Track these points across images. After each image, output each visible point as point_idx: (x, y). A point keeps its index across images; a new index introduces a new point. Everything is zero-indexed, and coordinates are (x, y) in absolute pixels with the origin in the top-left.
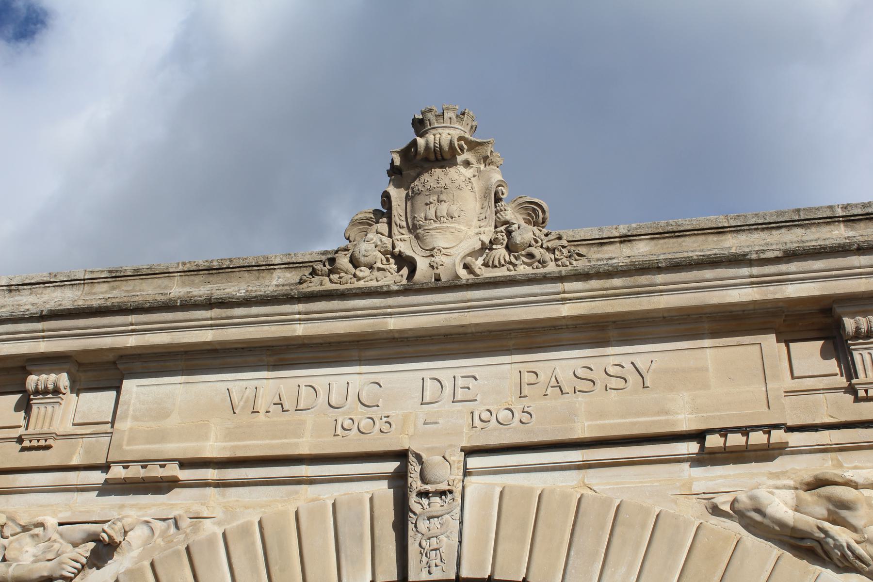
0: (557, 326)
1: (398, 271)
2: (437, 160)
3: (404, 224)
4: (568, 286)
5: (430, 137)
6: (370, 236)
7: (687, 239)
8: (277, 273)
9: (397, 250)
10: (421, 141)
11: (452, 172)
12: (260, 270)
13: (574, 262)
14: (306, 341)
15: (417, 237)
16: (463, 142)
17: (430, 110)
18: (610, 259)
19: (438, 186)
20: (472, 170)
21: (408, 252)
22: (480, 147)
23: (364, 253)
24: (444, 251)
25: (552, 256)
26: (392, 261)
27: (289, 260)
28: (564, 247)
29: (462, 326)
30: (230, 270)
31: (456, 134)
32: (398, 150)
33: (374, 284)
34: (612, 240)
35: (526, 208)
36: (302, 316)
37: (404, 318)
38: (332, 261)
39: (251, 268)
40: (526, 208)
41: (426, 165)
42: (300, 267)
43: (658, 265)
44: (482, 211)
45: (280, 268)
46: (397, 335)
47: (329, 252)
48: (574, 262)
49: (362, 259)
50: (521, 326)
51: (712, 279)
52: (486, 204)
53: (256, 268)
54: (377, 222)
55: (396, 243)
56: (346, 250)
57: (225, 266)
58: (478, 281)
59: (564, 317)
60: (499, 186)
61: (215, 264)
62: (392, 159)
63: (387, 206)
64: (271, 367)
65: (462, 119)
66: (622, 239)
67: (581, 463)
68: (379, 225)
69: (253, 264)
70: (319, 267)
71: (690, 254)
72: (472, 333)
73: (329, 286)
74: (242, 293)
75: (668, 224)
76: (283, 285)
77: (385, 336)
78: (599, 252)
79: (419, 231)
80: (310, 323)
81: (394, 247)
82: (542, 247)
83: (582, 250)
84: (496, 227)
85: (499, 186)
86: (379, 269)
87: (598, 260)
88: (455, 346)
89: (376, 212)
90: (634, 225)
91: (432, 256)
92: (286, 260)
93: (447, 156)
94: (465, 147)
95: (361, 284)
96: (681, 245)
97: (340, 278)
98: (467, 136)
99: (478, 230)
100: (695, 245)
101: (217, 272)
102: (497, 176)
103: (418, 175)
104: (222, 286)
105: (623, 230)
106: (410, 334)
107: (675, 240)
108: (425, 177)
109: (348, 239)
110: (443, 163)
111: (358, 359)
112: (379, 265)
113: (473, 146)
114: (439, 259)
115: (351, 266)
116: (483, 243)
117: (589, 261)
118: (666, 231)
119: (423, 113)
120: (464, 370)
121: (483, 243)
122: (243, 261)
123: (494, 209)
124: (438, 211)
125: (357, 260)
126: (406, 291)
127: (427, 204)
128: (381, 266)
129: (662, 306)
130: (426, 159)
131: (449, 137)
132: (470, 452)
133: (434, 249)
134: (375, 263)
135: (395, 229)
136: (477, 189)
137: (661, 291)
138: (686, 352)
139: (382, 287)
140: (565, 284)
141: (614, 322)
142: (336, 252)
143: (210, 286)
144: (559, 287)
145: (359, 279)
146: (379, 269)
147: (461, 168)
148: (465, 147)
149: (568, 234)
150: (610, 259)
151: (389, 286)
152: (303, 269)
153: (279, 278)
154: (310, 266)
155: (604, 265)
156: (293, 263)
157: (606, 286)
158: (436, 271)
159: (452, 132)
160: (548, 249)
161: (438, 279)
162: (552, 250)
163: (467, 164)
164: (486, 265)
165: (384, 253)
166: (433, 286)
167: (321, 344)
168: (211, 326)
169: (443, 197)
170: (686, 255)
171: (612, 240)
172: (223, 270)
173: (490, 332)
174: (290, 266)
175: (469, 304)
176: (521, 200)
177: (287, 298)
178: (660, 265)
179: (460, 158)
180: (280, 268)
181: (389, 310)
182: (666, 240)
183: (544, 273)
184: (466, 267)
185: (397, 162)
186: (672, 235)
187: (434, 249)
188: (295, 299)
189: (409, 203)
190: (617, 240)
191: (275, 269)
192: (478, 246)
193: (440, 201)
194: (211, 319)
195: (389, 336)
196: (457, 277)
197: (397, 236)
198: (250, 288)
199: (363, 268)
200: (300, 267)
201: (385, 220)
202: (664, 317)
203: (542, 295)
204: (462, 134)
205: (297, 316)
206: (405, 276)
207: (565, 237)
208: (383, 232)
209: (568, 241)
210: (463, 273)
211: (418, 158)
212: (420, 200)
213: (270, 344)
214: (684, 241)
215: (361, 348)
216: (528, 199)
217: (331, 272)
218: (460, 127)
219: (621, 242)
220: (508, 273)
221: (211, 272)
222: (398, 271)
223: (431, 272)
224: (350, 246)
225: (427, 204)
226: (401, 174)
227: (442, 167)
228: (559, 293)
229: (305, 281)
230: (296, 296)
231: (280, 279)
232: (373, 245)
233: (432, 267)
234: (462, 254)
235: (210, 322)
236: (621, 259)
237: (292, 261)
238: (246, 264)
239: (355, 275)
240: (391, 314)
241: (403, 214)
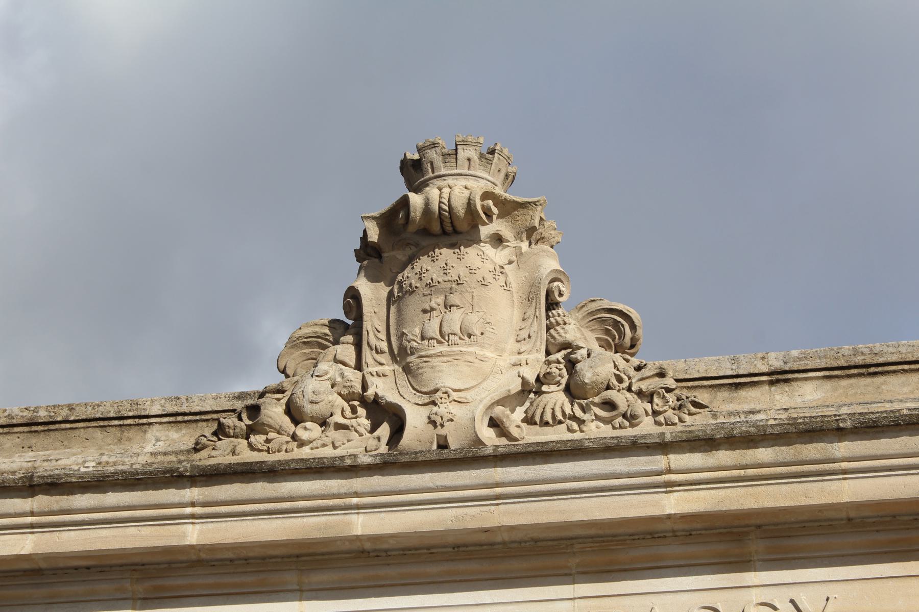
0: (657, 533)
1: (373, 430)
2: (444, 233)
3: (384, 346)
4: (677, 460)
5: (433, 192)
6: (323, 366)
7: (890, 379)
8: (155, 432)
9: (370, 393)
10: (416, 200)
11: (471, 254)
12: (123, 425)
13: (687, 418)
14: (203, 556)
15: (407, 370)
16: (490, 203)
17: (434, 145)
18: (752, 412)
19: (446, 278)
20: (506, 251)
21: (390, 396)
22: (521, 211)
23: (310, 396)
24: (454, 395)
25: (648, 407)
26: (362, 411)
27: (176, 409)
28: (669, 390)
29: (486, 530)
30: (68, 426)
31: (478, 187)
32: (375, 214)
33: (328, 452)
34: (756, 379)
35: (602, 321)
36: (198, 510)
37: (382, 515)
38: (254, 411)
39: (106, 423)
40: (602, 321)
41: (425, 242)
43: (838, 425)
44: (524, 325)
45: (161, 423)
46: (368, 546)
47: (250, 395)
48: (687, 418)
49: (308, 408)
50: (592, 532)
51: (771, 463)
52: (530, 312)
53: (116, 422)
54: (336, 342)
55: (369, 379)
56: (280, 390)
57: (59, 419)
58: (515, 449)
59: (669, 517)
60: (554, 280)
61: (43, 415)
62: (365, 231)
63: (354, 315)
64: (139, 602)
65: (490, 161)
66: (774, 378)
68: (339, 348)
69: (112, 415)
70: (230, 421)
71: (896, 406)
72: (504, 543)
73: (246, 456)
74: (90, 467)
75: (856, 352)
76: (165, 454)
77: (347, 546)
78: (731, 400)
79: (411, 359)
80: (212, 522)
81: (365, 387)
82: (629, 389)
83: (702, 397)
84: (548, 353)
85: (554, 280)
86: (339, 427)
87: (731, 414)
88: (474, 566)
89: (334, 324)
90: (795, 353)
91: (434, 403)
92: (170, 408)
93: (463, 226)
94: (495, 210)
95: (305, 452)
97: (268, 441)
98: (499, 191)
99: (515, 358)
100: (905, 390)
101: (46, 428)
102: (550, 263)
103: (411, 260)
104: (53, 454)
105: (775, 361)
106: (392, 543)
107: (869, 380)
108: (423, 262)
109: (283, 371)
110: (454, 239)
111: (297, 587)
112: (338, 418)
113: (508, 208)
114: (445, 409)
115: (287, 419)
116: (524, 382)
117: (715, 416)
118: (852, 363)
119: (420, 150)
121: (524, 382)
123: (544, 322)
124: (445, 324)
125: (299, 409)
126: (384, 467)
127: (425, 311)
128: (341, 420)
129: (846, 499)
130: (425, 232)
131: (466, 193)
133: (436, 391)
134: (331, 415)
135: (367, 355)
136: (514, 286)
137: (845, 472)
138: (891, 583)
139: (342, 458)
140: (671, 456)
141: (759, 527)
142: (262, 395)
143: (31, 454)
144: (659, 461)
145: (302, 444)
146: (339, 427)
147: (488, 249)
148: (495, 210)
149: (677, 367)
150: (752, 412)
151: (355, 456)
152: (200, 424)
153: (158, 440)
154: (214, 420)
155: (741, 424)
157: (744, 462)
158: (442, 432)
159: (471, 183)
160: (640, 393)
161: (443, 445)
162: (649, 397)
163: (498, 240)
164: (529, 420)
165: (348, 398)
166: (434, 457)
167: (231, 560)
168: (32, 526)
169: (454, 299)
170: (888, 407)
171: (756, 379)
172: (57, 426)
173: (536, 541)
174: (177, 418)
175: (499, 490)
176: (593, 306)
177: (172, 476)
178: (841, 425)
179: (485, 231)
180: (161, 423)
181: (355, 500)
182: (853, 381)
183: (634, 437)
184: (494, 423)
185: (374, 235)
186: (864, 370)
187: (436, 391)
188: (185, 480)
189: (393, 309)
190: (764, 378)
191: (150, 424)
192: (516, 386)
193: (448, 306)
194: (32, 514)
195: (356, 546)
196: (478, 442)
197: (371, 367)
198: (105, 459)
199: (309, 424)
200: (197, 421)
201: (349, 338)
202: (849, 520)
203: (629, 475)
204: (489, 187)
205: (189, 510)
206: (385, 440)
207: (670, 373)
208: (347, 360)
209: (677, 381)
210: (488, 435)
211: (411, 228)
212: (413, 304)
213: (137, 560)
214: (885, 383)
215: (304, 568)
216: (606, 304)
217: (251, 430)
218: (485, 175)
219: (771, 383)
220: (569, 436)
221: (34, 428)
222: (373, 430)
223: (431, 433)
224: (287, 384)
225: (425, 311)
226: (380, 257)
227: (452, 246)
228: (660, 473)
229: (204, 447)
230: (188, 474)
232: (328, 384)
233: (433, 423)
234: (487, 401)
235: (29, 520)
236: (772, 414)
237: (182, 411)
238: (98, 415)
239: (294, 437)
240: (358, 507)
241: (382, 328)
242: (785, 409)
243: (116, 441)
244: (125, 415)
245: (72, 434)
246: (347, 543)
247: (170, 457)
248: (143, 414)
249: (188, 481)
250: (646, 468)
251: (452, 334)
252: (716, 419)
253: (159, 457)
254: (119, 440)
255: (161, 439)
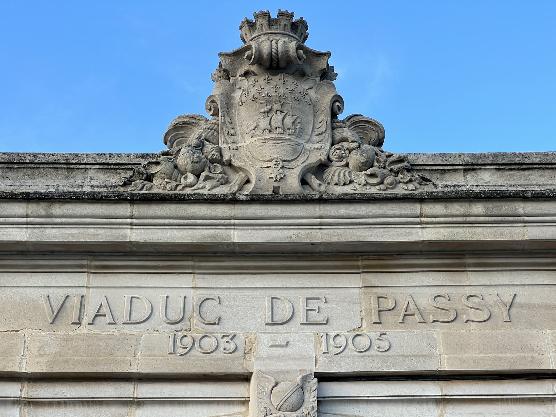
0: (423, 251)
12: (69, 168)
19: (276, 94)
29: (313, 244)
30: (33, 166)
37: (250, 231)
39: (58, 166)
42: (117, 169)
43: (524, 194)
47: (149, 155)
50: (374, 249)
57: (27, 161)
66: (467, 167)
67: (440, 397)
77: (225, 248)
83: (428, 176)
96: (528, 178)
100: (543, 179)
107: (521, 173)
118: (512, 162)
120: (310, 291)
122: (49, 157)
132: (323, 378)
143: (10, 181)
152: (118, 171)
154: (131, 169)
156: (108, 164)
178: (525, 195)
181: (233, 221)
200: (117, 169)
219: (465, 170)
221: (11, 166)
231: (94, 181)
240: (234, 225)
242: (477, 185)
243: (65, 177)
244: (71, 162)
245: (35, 171)
246: (225, 247)
247: (103, 189)
248: (82, 162)
249: (129, 203)
250: (410, 213)
251: (278, 127)
252: (437, 189)
253: (96, 189)
254: (66, 177)
255: (94, 178)
